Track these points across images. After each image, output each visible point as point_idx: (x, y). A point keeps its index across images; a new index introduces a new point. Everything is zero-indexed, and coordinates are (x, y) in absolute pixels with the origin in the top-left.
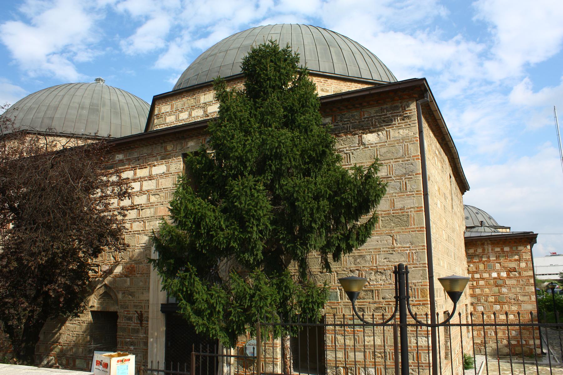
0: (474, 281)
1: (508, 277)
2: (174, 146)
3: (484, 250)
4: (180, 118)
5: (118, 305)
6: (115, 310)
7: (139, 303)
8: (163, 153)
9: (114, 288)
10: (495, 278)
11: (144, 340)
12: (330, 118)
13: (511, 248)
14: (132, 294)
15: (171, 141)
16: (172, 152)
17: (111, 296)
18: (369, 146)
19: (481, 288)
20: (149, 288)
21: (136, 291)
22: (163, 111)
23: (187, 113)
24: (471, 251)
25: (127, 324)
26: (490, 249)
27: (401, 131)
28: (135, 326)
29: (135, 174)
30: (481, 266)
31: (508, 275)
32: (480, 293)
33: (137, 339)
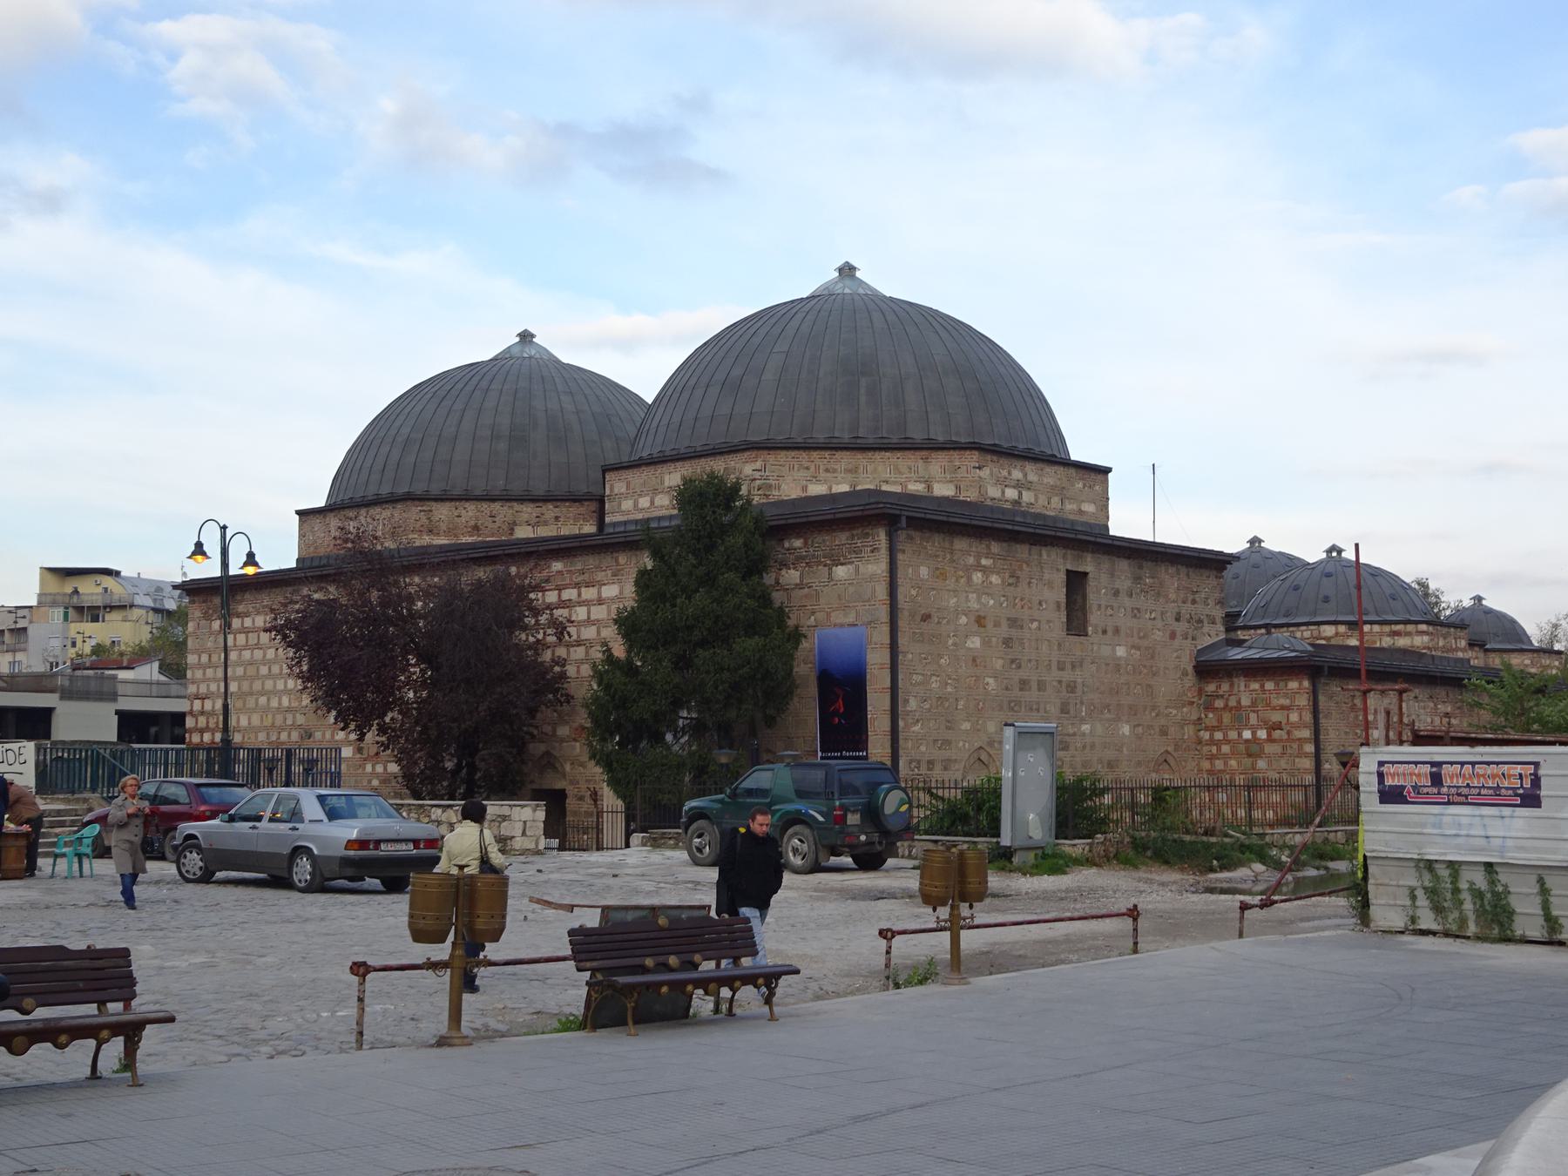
0: (1214, 745)
1: (1270, 739)
3: (1232, 685)
4: (640, 506)
6: (562, 787)
10: (1247, 741)
12: (802, 540)
13: (1277, 684)
18: (839, 583)
19: (1226, 758)
22: (616, 491)
23: (648, 498)
24: (1211, 688)
26: (1242, 684)
27: (870, 566)
29: (579, 595)
30: (1227, 717)
31: (1269, 735)
32: (1222, 767)
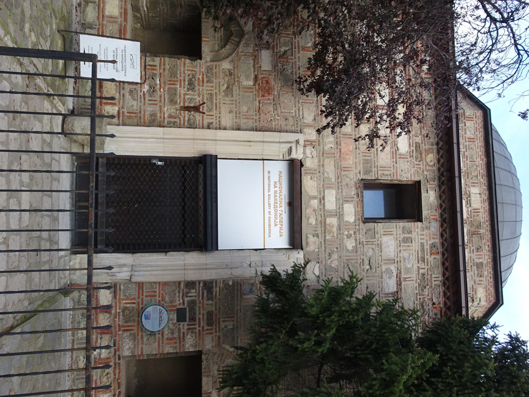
2: (432, 166)
5: (211, 61)
6: (203, 55)
7: (216, 104)
8: (424, 147)
9: (238, 53)
11: (158, 115)
14: (229, 90)
15: (439, 161)
16: (425, 163)
17: (225, 46)
20: (239, 129)
21: (234, 98)
25: (182, 78)
28: (180, 96)
33: (161, 100)
